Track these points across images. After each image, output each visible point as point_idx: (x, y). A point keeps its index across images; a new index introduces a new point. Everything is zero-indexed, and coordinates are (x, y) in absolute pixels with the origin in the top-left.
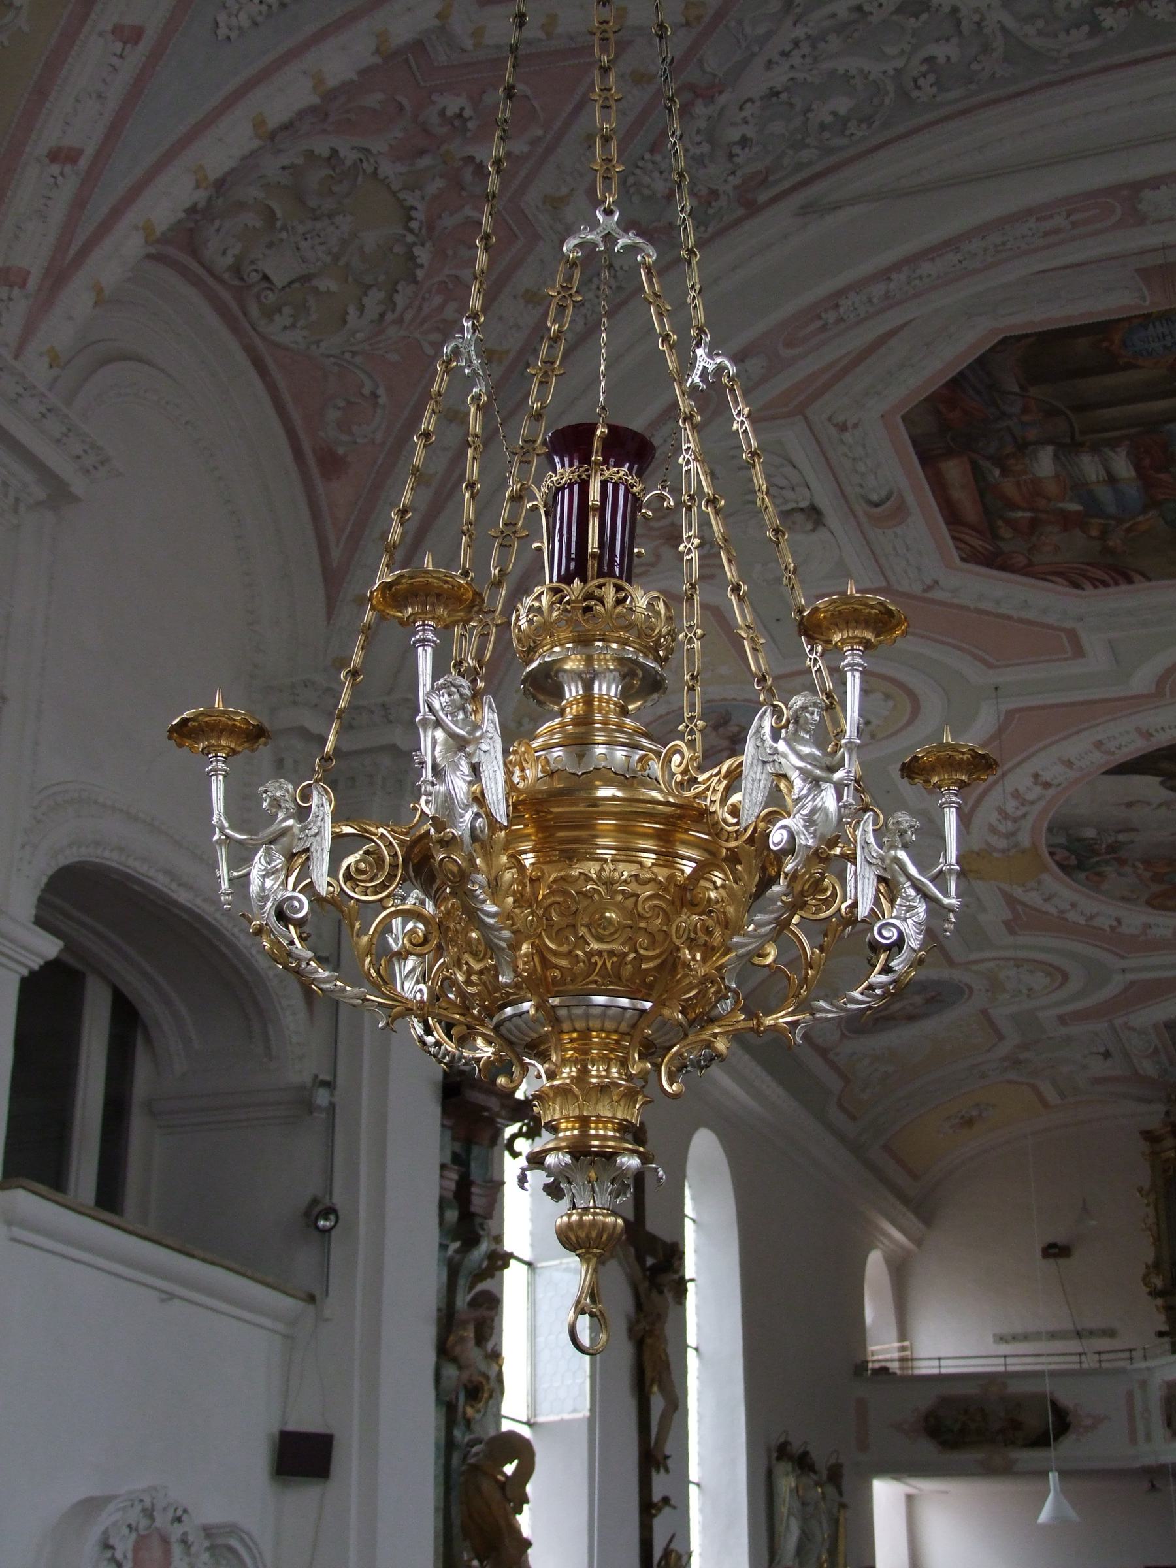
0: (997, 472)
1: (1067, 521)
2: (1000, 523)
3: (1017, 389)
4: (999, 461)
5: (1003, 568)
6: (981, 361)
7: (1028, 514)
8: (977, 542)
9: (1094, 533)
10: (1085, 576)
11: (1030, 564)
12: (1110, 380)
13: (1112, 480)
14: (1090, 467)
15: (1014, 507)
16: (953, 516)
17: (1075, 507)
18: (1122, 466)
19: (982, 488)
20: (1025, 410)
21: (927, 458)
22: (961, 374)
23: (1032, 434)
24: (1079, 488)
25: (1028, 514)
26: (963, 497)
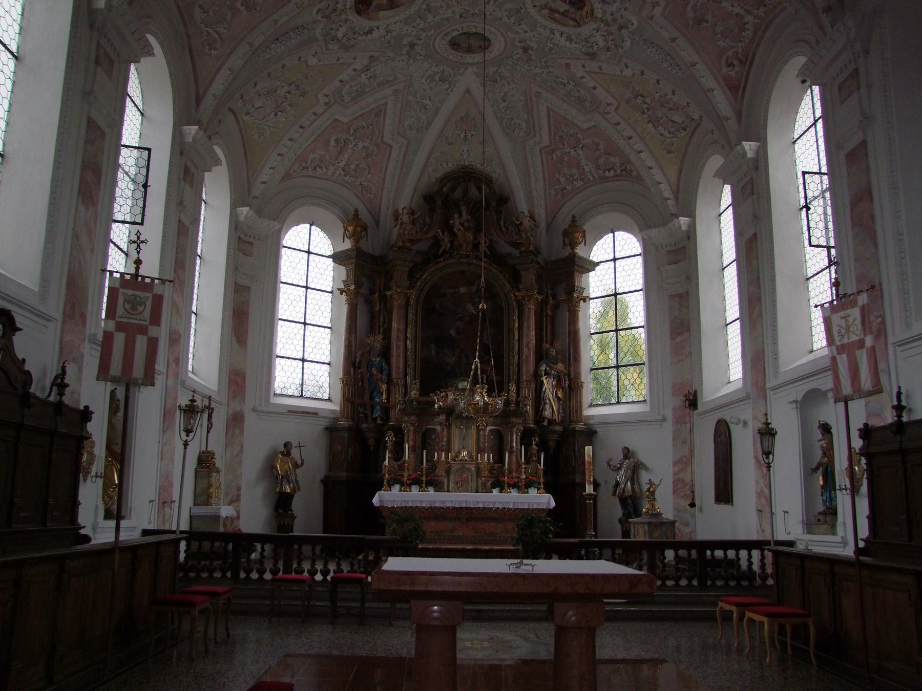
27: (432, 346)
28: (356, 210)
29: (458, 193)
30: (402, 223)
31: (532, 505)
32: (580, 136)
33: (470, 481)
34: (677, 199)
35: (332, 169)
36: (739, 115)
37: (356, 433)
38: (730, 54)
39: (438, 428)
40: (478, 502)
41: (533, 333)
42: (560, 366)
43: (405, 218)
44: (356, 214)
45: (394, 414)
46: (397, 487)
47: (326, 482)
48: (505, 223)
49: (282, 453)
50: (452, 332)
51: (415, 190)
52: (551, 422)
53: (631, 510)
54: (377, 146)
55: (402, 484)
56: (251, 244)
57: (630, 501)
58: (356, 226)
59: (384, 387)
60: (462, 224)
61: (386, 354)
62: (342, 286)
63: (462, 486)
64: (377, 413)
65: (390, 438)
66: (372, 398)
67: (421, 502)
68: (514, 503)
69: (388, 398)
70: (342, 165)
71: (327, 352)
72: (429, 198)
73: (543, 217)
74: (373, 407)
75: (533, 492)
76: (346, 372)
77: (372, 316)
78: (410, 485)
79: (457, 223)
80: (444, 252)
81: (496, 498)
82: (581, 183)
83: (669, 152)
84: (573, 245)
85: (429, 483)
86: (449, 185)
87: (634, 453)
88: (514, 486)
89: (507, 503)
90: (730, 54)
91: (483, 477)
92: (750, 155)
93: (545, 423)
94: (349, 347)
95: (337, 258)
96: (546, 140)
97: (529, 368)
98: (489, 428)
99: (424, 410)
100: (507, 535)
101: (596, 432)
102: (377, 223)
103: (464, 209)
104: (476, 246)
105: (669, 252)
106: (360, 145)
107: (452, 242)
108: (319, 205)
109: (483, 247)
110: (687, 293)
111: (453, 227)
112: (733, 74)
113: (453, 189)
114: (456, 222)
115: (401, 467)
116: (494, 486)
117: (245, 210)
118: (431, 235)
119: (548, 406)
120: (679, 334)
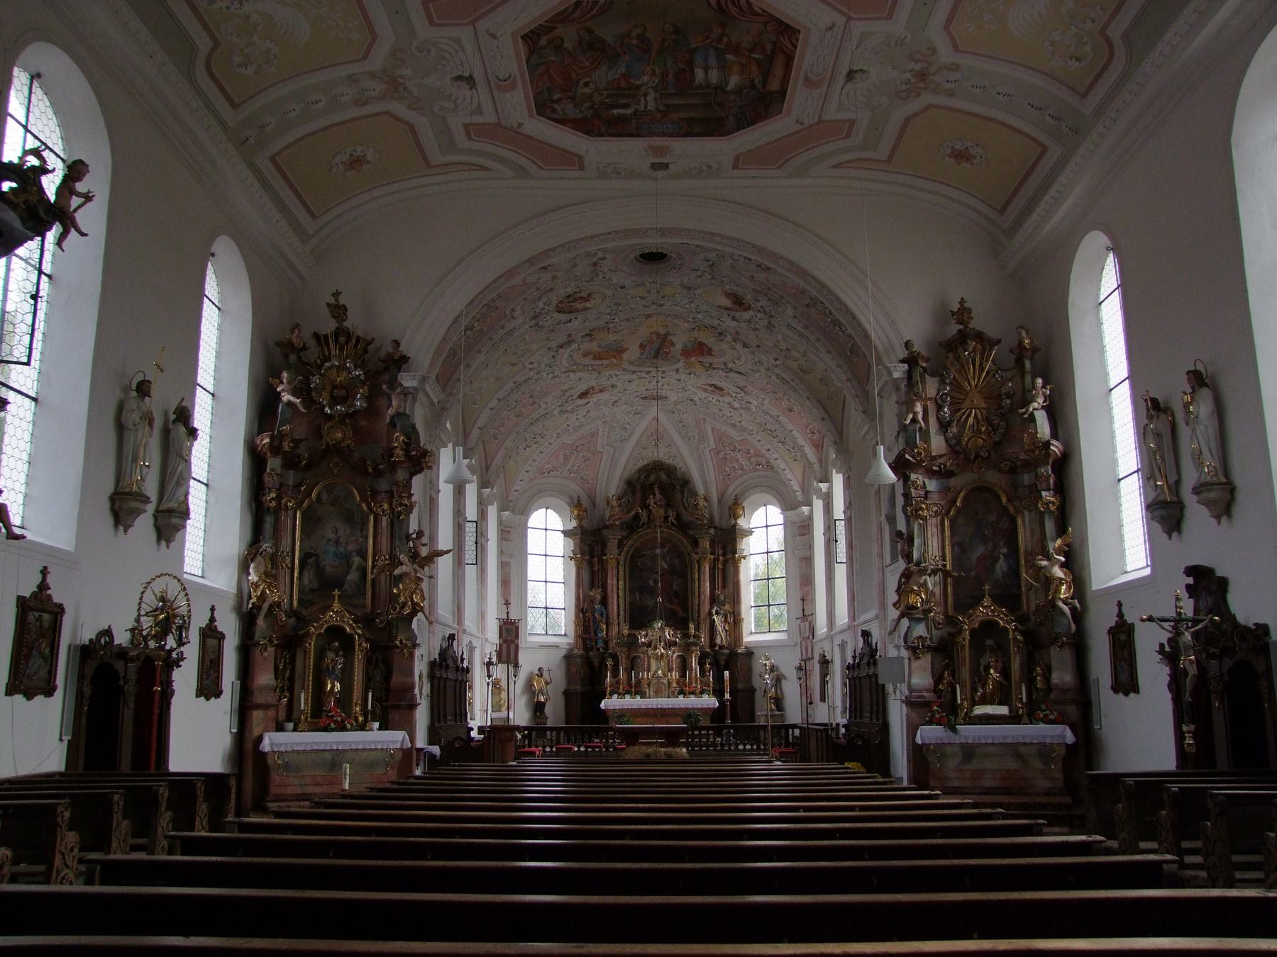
0: (756, 81)
1: (736, 49)
2: (769, 53)
3: (730, 117)
4: (753, 86)
5: (781, 23)
6: (739, 129)
7: (752, 55)
8: (786, 43)
9: (725, 39)
10: (742, 10)
11: (766, 24)
12: (692, 115)
13: (706, 69)
14: (714, 76)
15: (758, 62)
16: (789, 59)
17: (729, 57)
18: (699, 74)
19: (766, 75)
20: (731, 108)
21: (782, 94)
22: (748, 126)
23: (732, 97)
24: (724, 67)
25: (752, 55)
26: (778, 71)
27: (637, 593)
28: (579, 497)
29: (652, 478)
30: (612, 507)
32: (736, 445)
34: (803, 491)
35: (560, 471)
36: (820, 461)
37: (587, 661)
38: (811, 427)
39: (642, 655)
41: (708, 584)
42: (727, 607)
43: (615, 503)
44: (579, 501)
45: (612, 644)
46: (616, 696)
47: (567, 694)
48: (687, 500)
49: (537, 675)
50: (651, 582)
51: (621, 479)
52: (721, 647)
54: (593, 453)
55: (619, 694)
56: (509, 532)
58: (579, 511)
59: (604, 627)
60: (655, 503)
61: (604, 602)
62: (572, 555)
63: (658, 694)
64: (600, 644)
65: (609, 663)
66: (596, 633)
67: (632, 705)
69: (607, 634)
70: (568, 468)
71: (562, 601)
72: (631, 484)
73: (715, 494)
74: (596, 640)
75: (705, 697)
76: (577, 616)
77: (593, 573)
78: (624, 695)
79: (652, 502)
80: (643, 524)
81: (681, 702)
82: (740, 471)
83: (795, 460)
84: (736, 517)
85: (636, 693)
86: (644, 475)
87: (777, 668)
88: (692, 693)
90: (811, 427)
92: (824, 490)
93: (717, 648)
94: (578, 598)
95: (566, 533)
96: (713, 445)
97: (703, 614)
98: (675, 655)
99: (631, 643)
101: (753, 653)
102: (594, 504)
103: (657, 492)
104: (666, 518)
105: (800, 527)
106: (581, 455)
107: (649, 516)
108: (552, 496)
109: (672, 519)
110: (810, 557)
111: (649, 505)
112: (815, 438)
113: (648, 476)
114: (651, 501)
115: (618, 682)
116: (680, 693)
117: (507, 513)
118: (633, 513)
119: (719, 637)
120: (806, 586)
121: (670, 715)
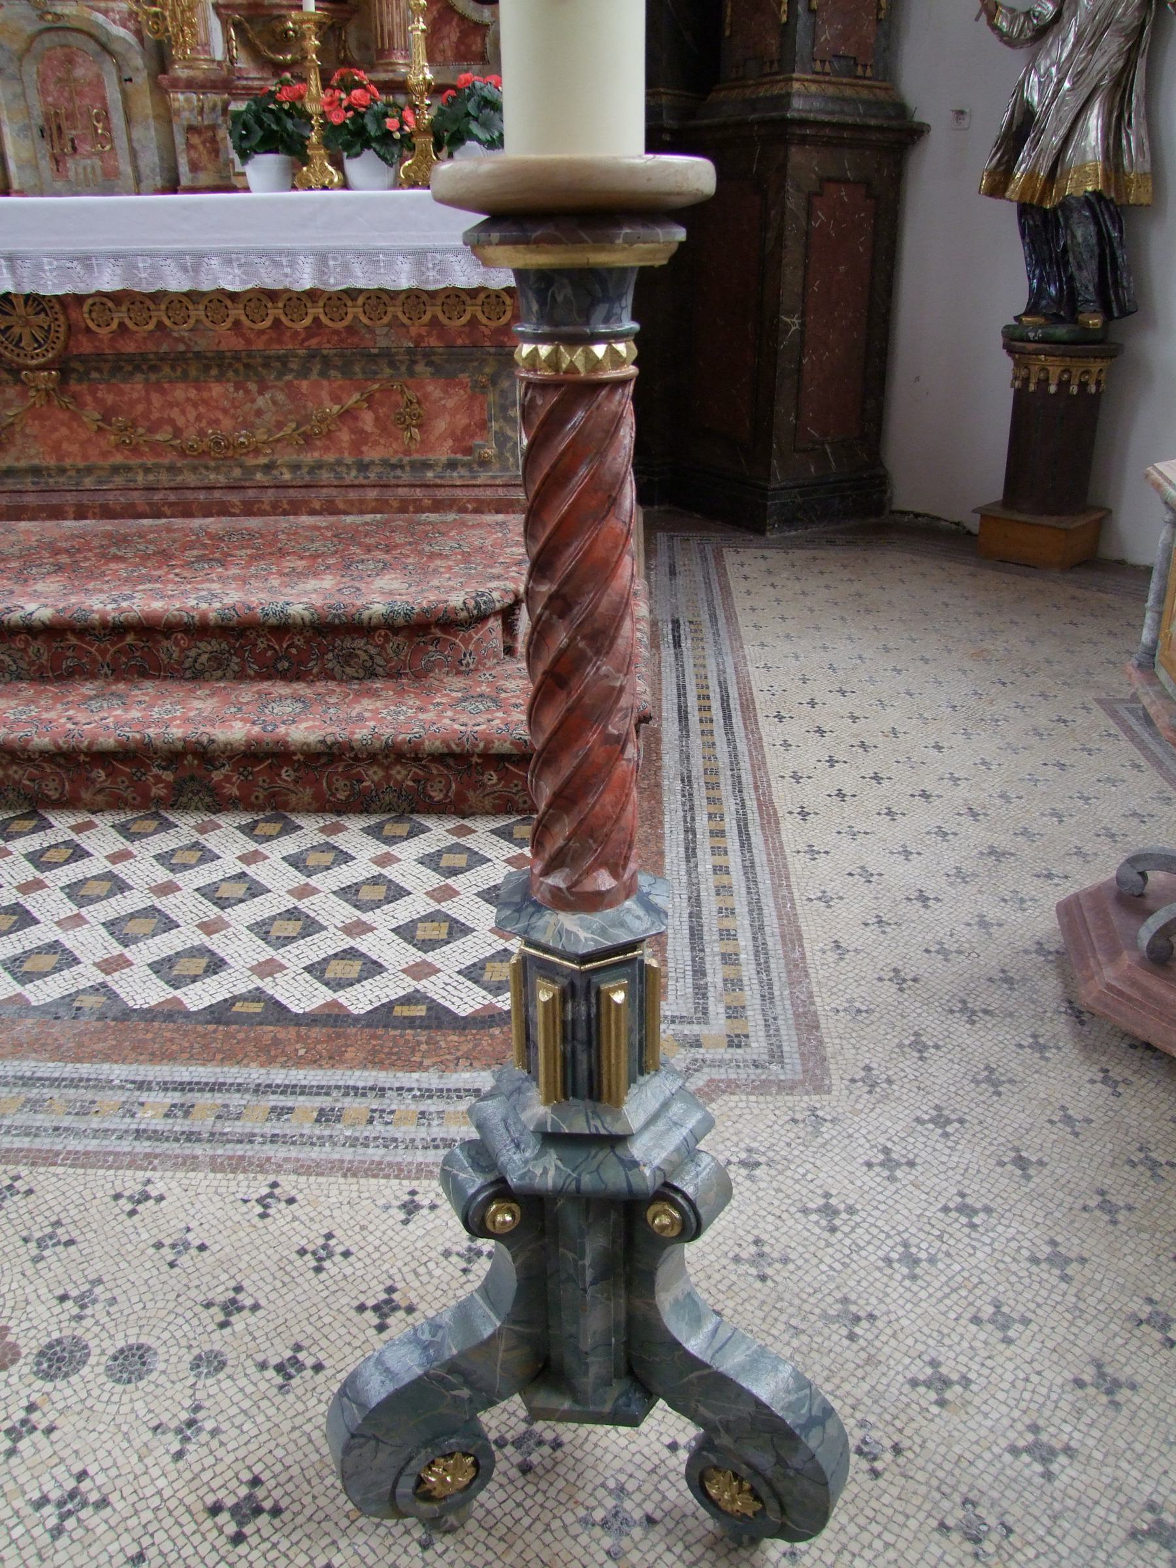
31: (443, 271)
33: (117, 119)
40: (85, 259)
53: (1086, 278)
57: (1082, 232)
68: (321, 257)
89: (272, 256)
91: (190, 85)
100: (310, 457)
121: (140, 364)
